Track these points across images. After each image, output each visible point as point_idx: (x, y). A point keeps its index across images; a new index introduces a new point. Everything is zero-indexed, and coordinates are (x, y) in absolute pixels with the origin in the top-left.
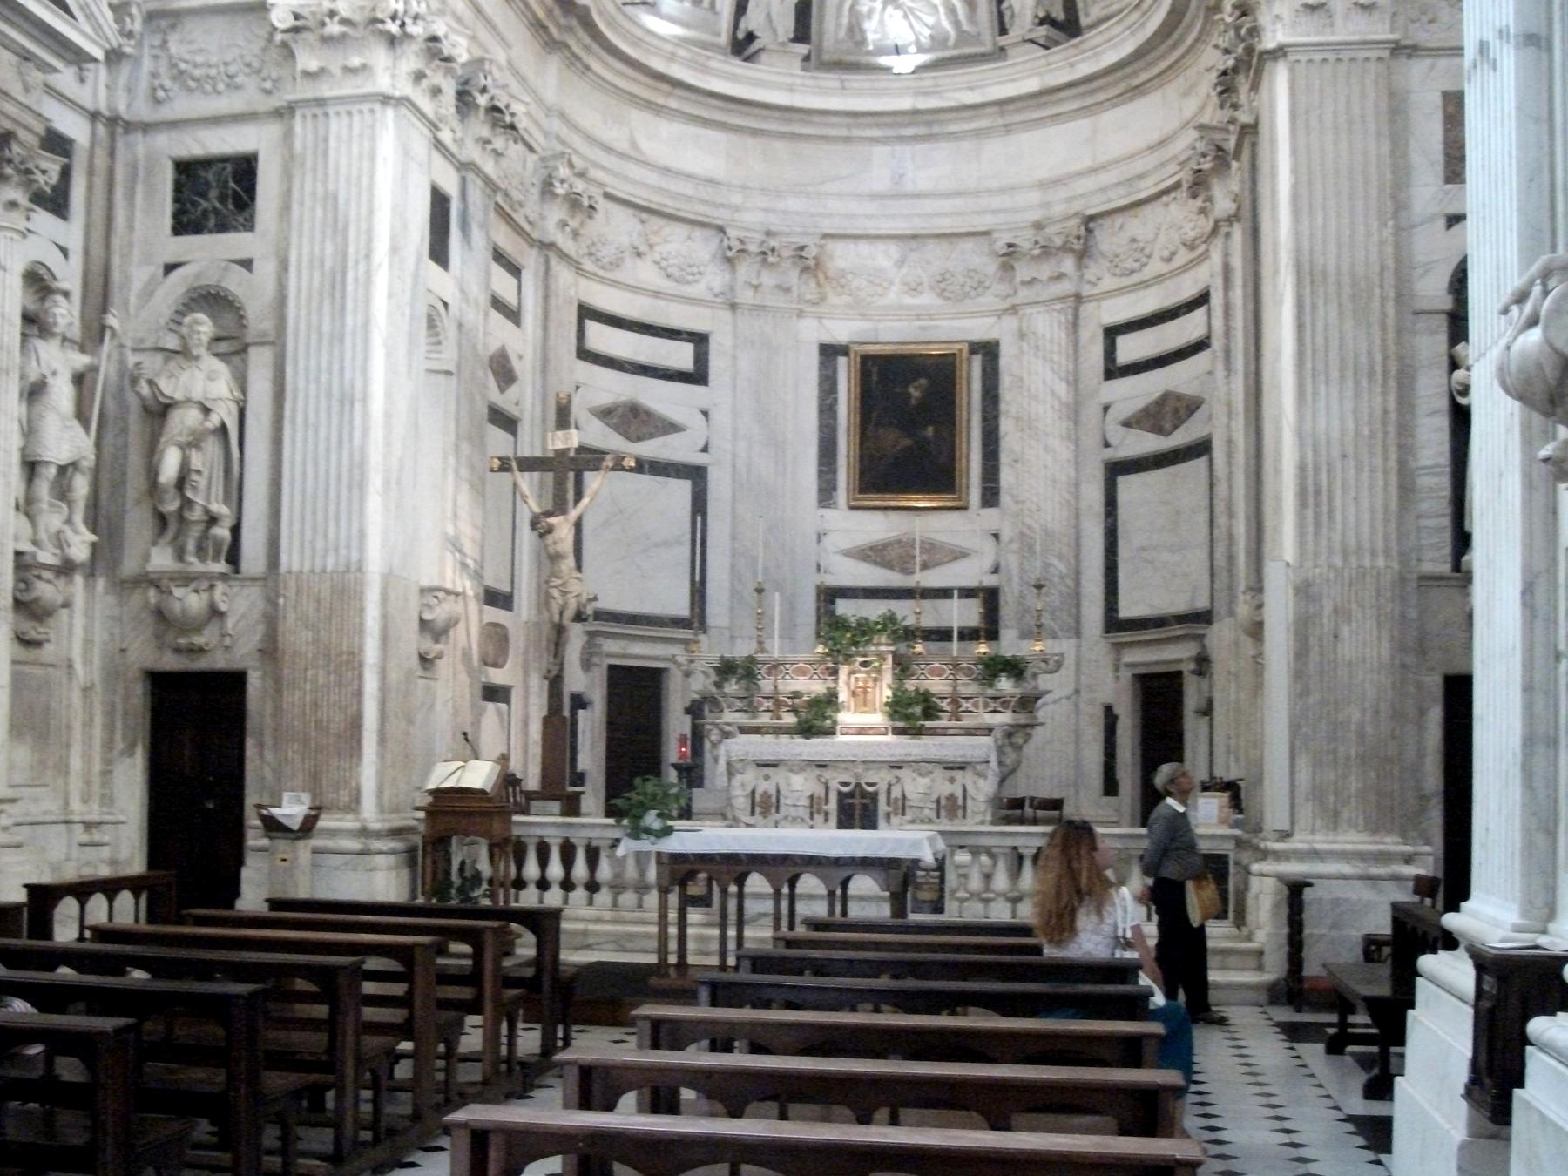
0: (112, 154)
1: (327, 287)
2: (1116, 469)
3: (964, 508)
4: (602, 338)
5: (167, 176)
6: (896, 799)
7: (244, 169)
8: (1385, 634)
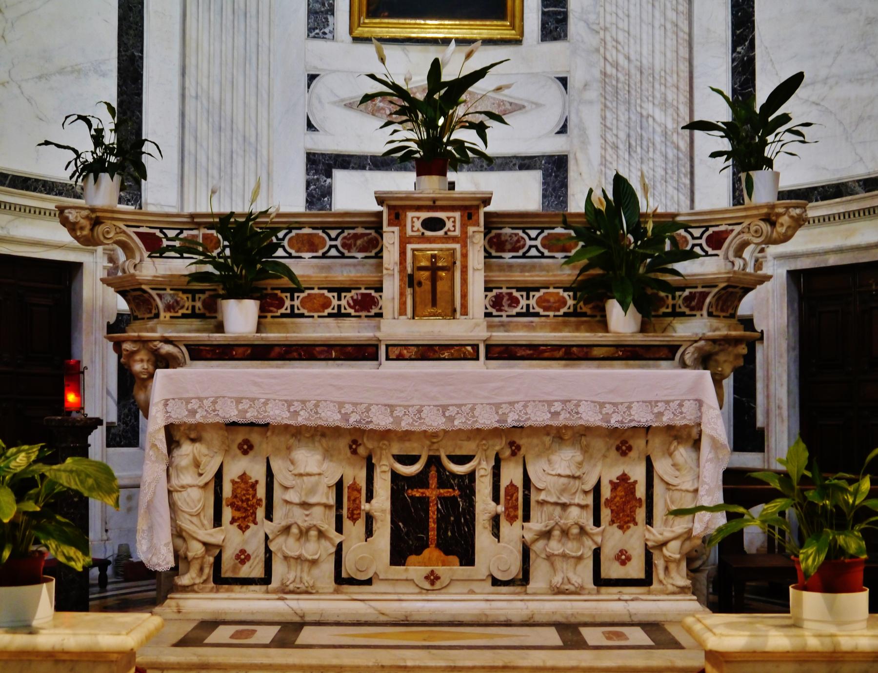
3: (518, 42)
6: (512, 486)
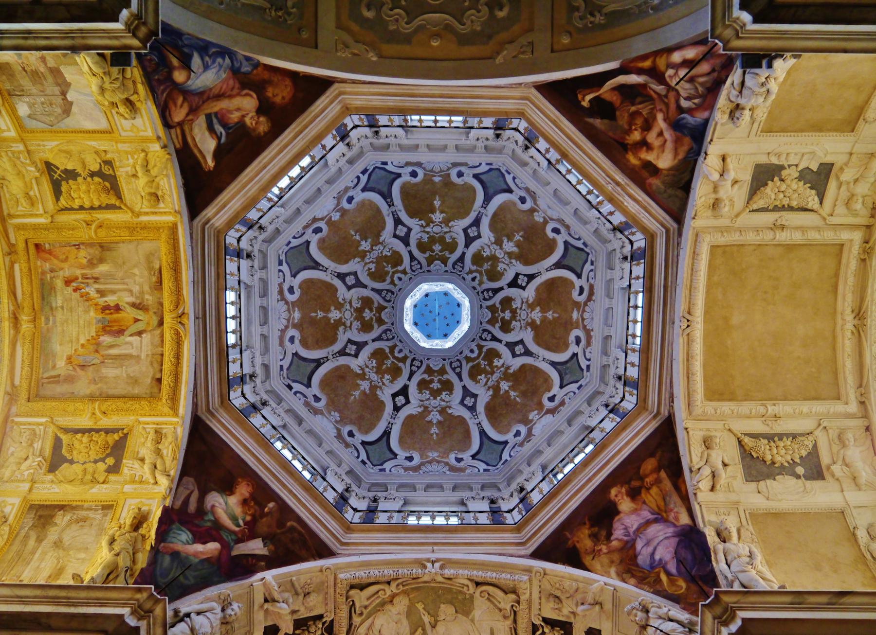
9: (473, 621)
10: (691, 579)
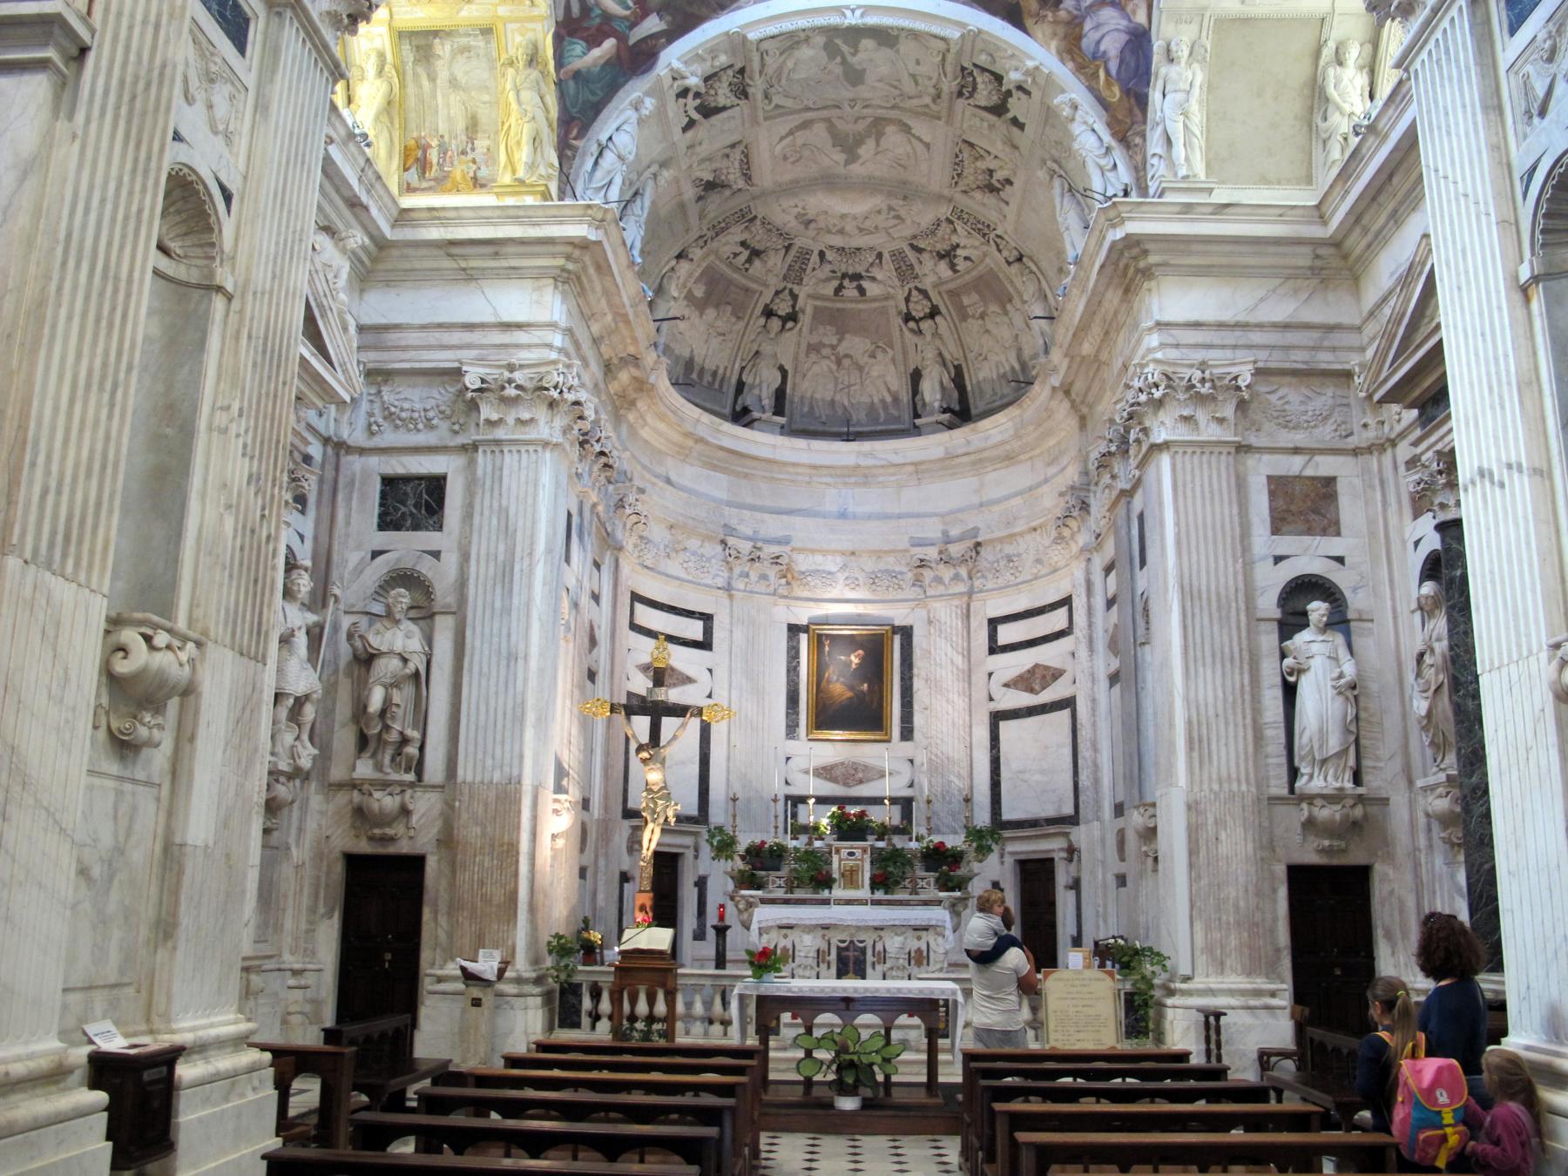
0: (337, 469)
1: (500, 574)
2: (997, 717)
3: (889, 741)
4: (647, 617)
5: (377, 486)
7: (436, 485)
8: (1250, 837)
9: (897, 51)
10: (1127, 92)
